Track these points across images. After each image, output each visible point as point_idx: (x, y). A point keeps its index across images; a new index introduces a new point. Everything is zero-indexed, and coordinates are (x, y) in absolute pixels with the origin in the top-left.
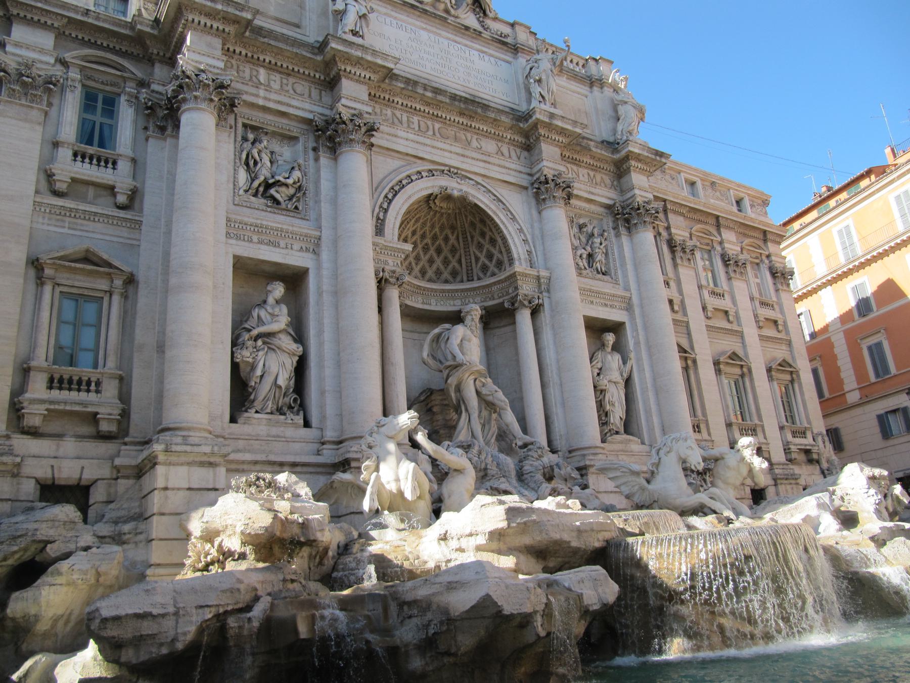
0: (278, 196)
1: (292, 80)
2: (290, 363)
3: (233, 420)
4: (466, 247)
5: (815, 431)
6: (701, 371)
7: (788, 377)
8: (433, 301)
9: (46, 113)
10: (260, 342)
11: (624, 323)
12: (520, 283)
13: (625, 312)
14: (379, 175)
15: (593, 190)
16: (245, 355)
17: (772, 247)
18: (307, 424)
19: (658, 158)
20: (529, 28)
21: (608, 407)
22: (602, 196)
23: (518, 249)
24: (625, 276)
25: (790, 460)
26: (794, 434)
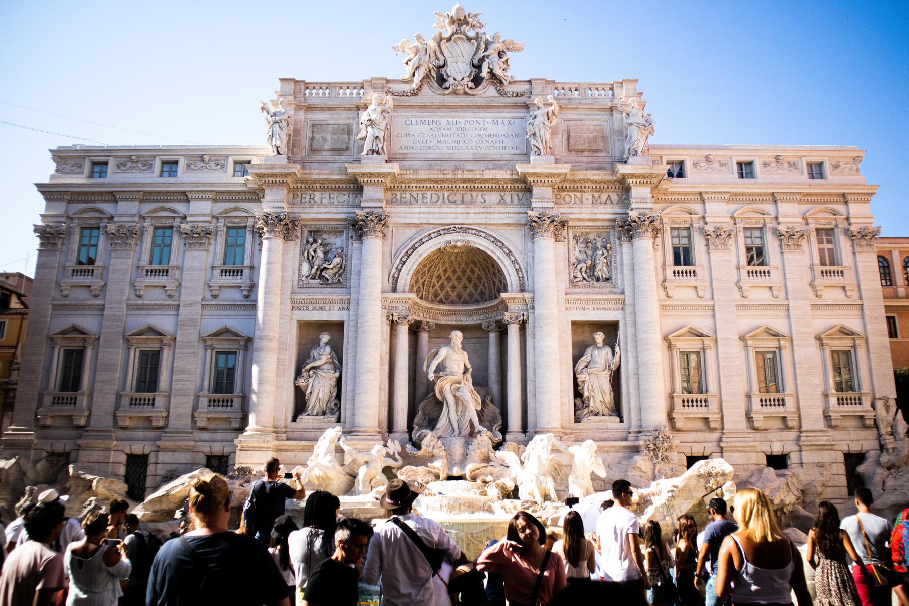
0: (327, 276)
3: (294, 419)
4: (486, 275)
8: (464, 318)
9: (208, 251)
10: (311, 372)
11: (618, 322)
13: (620, 312)
14: (397, 243)
15: (595, 210)
16: (302, 382)
17: (855, 209)
18: (339, 421)
21: (586, 394)
23: (511, 277)
24: (623, 280)
25: (831, 427)
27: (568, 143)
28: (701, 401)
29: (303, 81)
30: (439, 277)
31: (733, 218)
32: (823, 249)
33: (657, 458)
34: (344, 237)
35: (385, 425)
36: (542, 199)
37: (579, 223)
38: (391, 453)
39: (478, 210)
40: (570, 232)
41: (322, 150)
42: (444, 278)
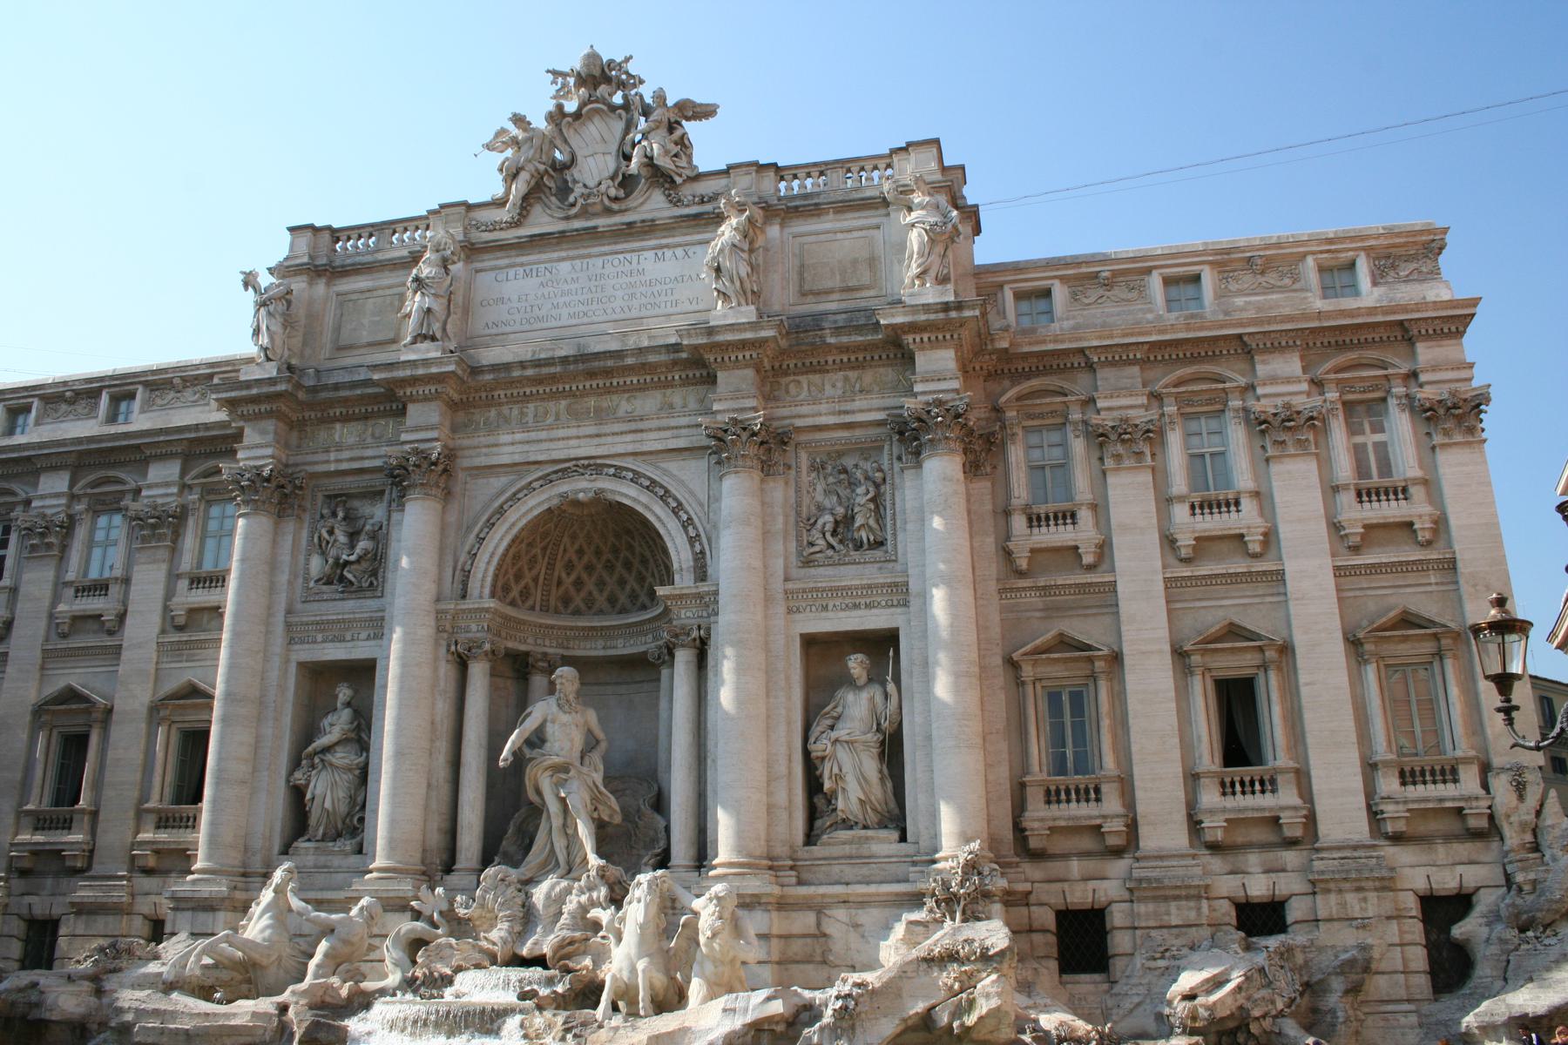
0: (350, 576)
1: (371, 422)
2: (344, 781)
5: (1497, 761)
6: (1130, 678)
7: (1428, 647)
8: (620, 643)
10: (317, 760)
12: (675, 610)
13: (899, 610)
15: (848, 406)
17: (1426, 353)
19: (953, 314)
20: (756, 164)
21: (827, 785)
22: (870, 410)
23: (680, 553)
26: (1408, 777)
27: (802, 279)
28: (1087, 791)
29: (329, 228)
30: (569, 567)
31: (1156, 397)
32: (1365, 445)
33: (953, 919)
34: (385, 504)
35: (437, 860)
36: (737, 395)
37: (818, 436)
38: (426, 911)
39: (617, 428)
40: (804, 456)
41: (350, 347)
42: (579, 568)
